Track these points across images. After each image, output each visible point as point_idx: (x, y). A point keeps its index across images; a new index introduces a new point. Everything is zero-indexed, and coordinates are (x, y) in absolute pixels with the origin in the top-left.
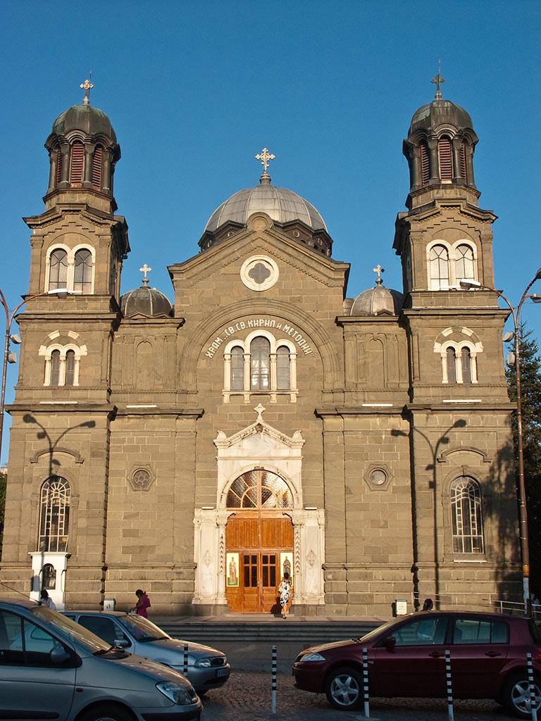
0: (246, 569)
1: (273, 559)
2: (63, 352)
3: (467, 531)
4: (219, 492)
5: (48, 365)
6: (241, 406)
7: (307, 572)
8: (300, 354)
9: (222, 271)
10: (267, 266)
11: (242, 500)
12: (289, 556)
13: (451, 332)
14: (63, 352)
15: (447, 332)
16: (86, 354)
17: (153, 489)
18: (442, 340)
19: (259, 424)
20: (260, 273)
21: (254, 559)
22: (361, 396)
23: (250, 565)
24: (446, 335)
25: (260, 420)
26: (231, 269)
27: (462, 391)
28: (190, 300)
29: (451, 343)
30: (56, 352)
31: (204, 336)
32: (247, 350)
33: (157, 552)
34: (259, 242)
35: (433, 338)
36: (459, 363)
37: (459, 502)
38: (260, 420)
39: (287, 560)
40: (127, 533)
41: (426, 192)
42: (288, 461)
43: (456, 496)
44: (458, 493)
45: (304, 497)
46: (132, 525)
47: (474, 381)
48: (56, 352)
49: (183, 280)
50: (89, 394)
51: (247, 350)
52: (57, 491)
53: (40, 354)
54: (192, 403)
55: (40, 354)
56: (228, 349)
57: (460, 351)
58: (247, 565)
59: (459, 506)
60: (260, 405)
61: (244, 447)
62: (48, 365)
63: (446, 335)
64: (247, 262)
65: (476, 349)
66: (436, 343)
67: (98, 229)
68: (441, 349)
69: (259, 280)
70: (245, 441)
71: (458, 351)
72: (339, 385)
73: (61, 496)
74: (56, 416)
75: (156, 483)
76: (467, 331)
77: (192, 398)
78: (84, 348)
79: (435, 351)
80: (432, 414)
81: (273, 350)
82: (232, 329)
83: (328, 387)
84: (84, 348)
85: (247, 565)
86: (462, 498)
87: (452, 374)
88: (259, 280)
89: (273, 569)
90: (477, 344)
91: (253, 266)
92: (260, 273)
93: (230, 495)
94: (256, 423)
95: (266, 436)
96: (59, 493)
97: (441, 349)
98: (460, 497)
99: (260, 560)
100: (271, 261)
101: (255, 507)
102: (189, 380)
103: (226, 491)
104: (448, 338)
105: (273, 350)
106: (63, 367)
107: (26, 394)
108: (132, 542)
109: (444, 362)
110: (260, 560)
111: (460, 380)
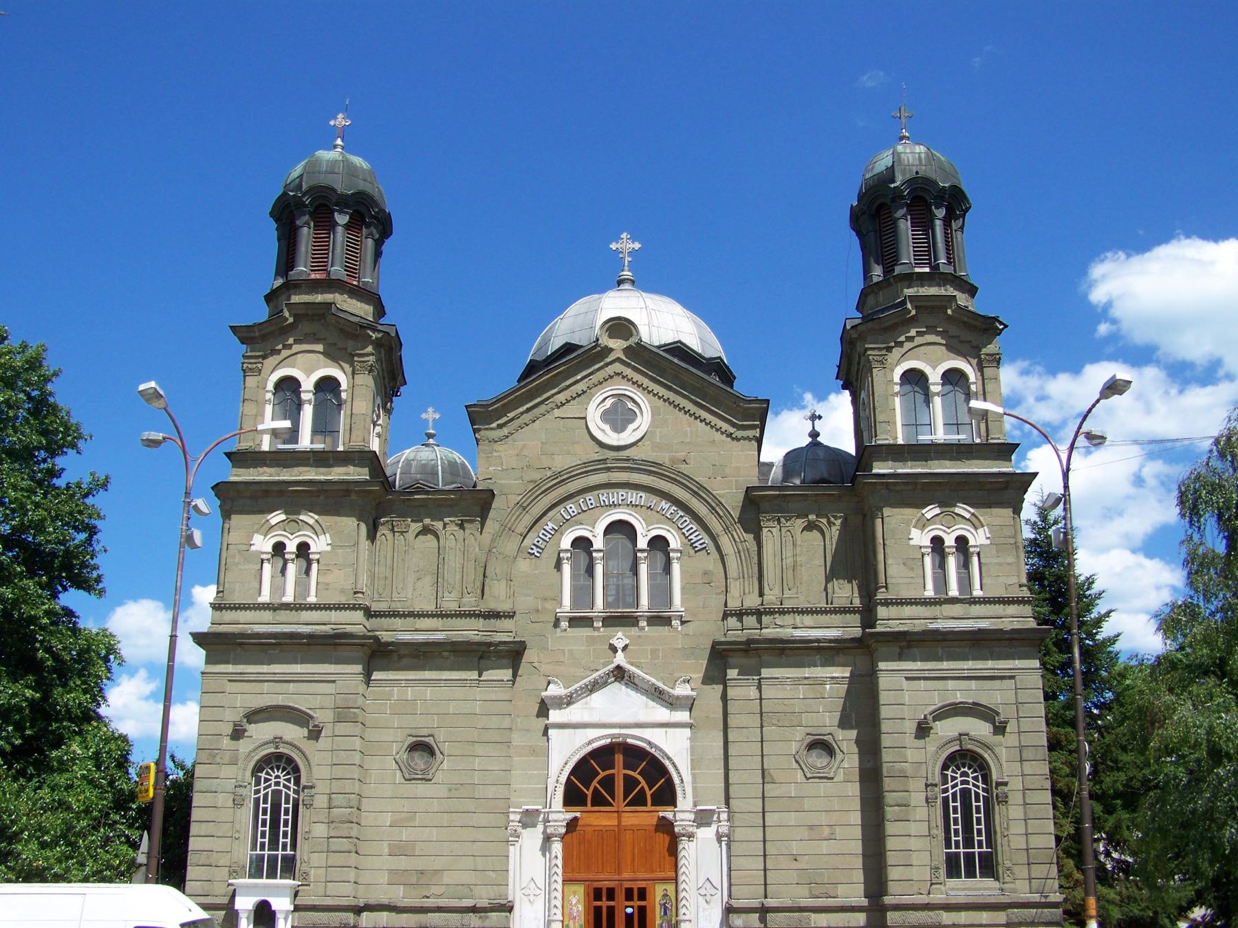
0: (598, 910)
1: (643, 894)
2: (291, 547)
3: (969, 842)
4: (551, 783)
6: (587, 636)
7: (701, 915)
9: (557, 413)
11: (589, 793)
12: (670, 888)
16: (329, 548)
17: (439, 777)
18: (923, 524)
19: (619, 667)
20: (619, 416)
21: (611, 894)
22: (788, 619)
23: (604, 903)
26: (571, 410)
27: (957, 609)
28: (504, 460)
31: (528, 519)
32: (598, 543)
33: (447, 878)
34: (618, 367)
35: (908, 523)
36: (952, 563)
37: (954, 794)
39: (665, 895)
40: (399, 850)
41: (890, 285)
42: (668, 729)
43: (950, 784)
44: (954, 778)
45: (694, 789)
46: (405, 834)
49: (492, 429)
50: (334, 616)
52: (277, 777)
54: (503, 632)
56: (566, 543)
57: (953, 543)
58: (598, 903)
59: (954, 800)
61: (593, 704)
65: (978, 538)
66: (913, 530)
67: (350, 344)
68: (921, 538)
69: (619, 428)
70: (595, 696)
71: (950, 541)
72: (752, 601)
73: (285, 786)
74: (277, 651)
75: (445, 766)
76: (963, 510)
77: (506, 624)
79: (912, 542)
80: (909, 647)
81: (642, 543)
82: (574, 509)
83: (734, 604)
85: (598, 903)
86: (960, 787)
87: (941, 581)
88: (619, 428)
89: (642, 911)
90: (981, 531)
91: (608, 403)
92: (619, 416)
93: (569, 785)
94: (611, 667)
96: (282, 781)
98: (956, 785)
99: (620, 895)
101: (612, 805)
102: (498, 598)
103: (563, 779)
105: (642, 543)
107: (229, 616)
108: (403, 863)
109: (928, 560)
110: (620, 895)
111: (954, 591)
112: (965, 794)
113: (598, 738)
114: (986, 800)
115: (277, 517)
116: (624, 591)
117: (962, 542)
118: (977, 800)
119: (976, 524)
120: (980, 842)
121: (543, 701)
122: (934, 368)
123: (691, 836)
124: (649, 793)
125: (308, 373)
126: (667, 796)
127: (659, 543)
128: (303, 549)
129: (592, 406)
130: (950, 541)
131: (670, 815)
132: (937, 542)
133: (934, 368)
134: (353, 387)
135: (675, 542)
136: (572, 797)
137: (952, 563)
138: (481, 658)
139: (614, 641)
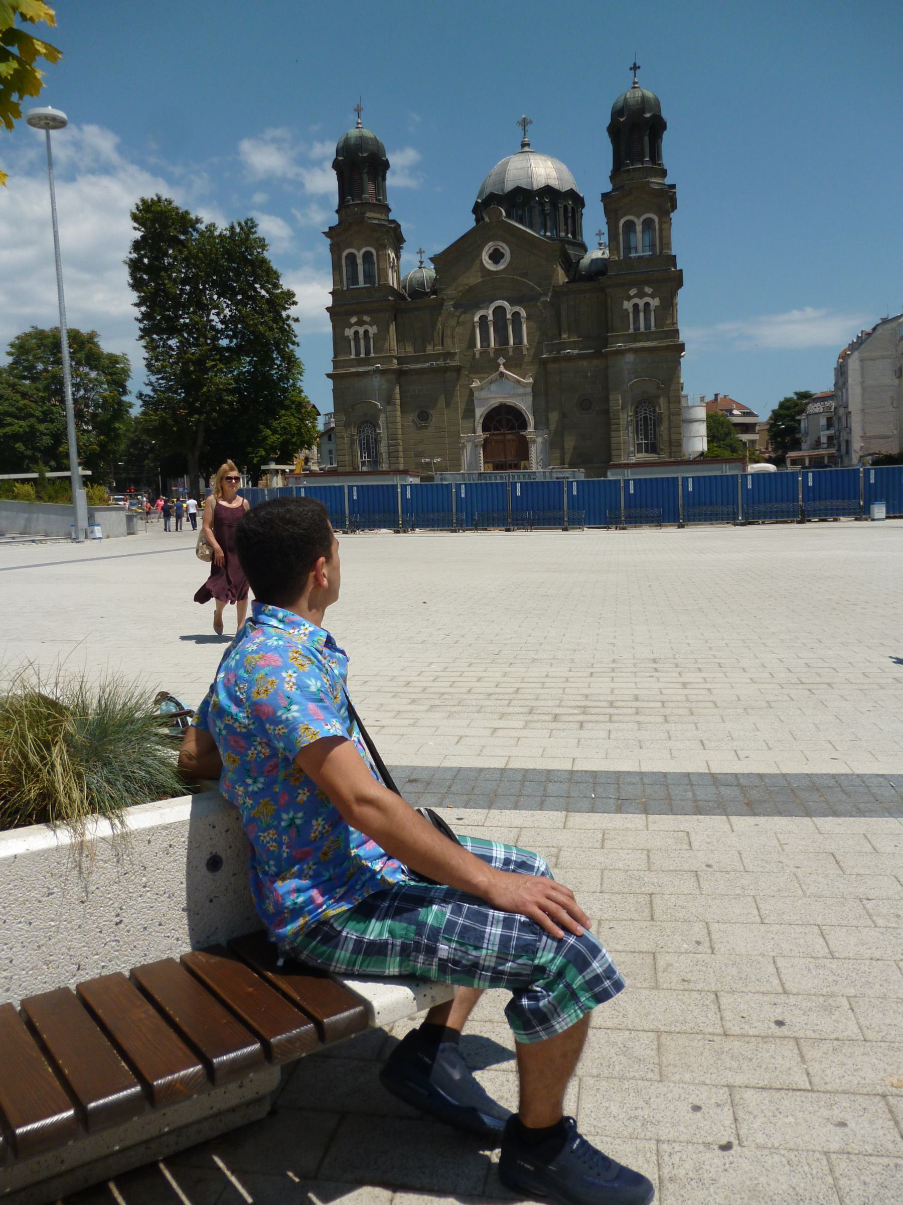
2: (361, 331)
5: (352, 343)
8: (528, 318)
10: (502, 250)
11: (492, 426)
12: (526, 462)
13: (636, 292)
14: (361, 331)
15: (633, 292)
18: (629, 298)
20: (496, 256)
24: (632, 294)
25: (502, 369)
29: (636, 300)
30: (356, 333)
36: (642, 315)
38: (502, 369)
47: (653, 329)
48: (356, 333)
51: (491, 318)
53: (346, 334)
55: (346, 334)
56: (476, 319)
59: (641, 421)
60: (501, 358)
61: (492, 389)
62: (352, 343)
63: (632, 294)
64: (486, 248)
70: (492, 385)
71: (641, 307)
76: (648, 290)
78: (375, 327)
81: (509, 316)
84: (375, 327)
91: (491, 251)
95: (507, 381)
97: (628, 305)
100: (504, 245)
103: (481, 421)
104: (634, 296)
105: (509, 316)
106: (362, 342)
109: (631, 315)
112: (645, 418)
113: (495, 403)
114: (654, 420)
115: (354, 320)
116: (502, 339)
117: (647, 305)
118: (651, 420)
119: (653, 296)
120: (651, 439)
121: (471, 389)
122: (639, 218)
123: (534, 441)
124: (516, 425)
125: (359, 250)
126: (524, 425)
127: (516, 315)
128: (366, 332)
129: (484, 254)
130: (641, 307)
131: (524, 433)
132: (636, 306)
133: (639, 218)
134: (378, 255)
135: (523, 313)
136: (485, 429)
137: (642, 315)
138: (445, 372)
139: (499, 361)
